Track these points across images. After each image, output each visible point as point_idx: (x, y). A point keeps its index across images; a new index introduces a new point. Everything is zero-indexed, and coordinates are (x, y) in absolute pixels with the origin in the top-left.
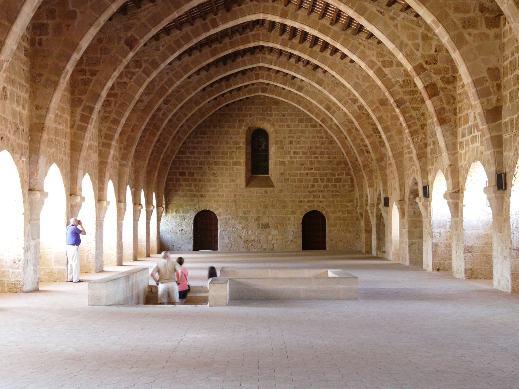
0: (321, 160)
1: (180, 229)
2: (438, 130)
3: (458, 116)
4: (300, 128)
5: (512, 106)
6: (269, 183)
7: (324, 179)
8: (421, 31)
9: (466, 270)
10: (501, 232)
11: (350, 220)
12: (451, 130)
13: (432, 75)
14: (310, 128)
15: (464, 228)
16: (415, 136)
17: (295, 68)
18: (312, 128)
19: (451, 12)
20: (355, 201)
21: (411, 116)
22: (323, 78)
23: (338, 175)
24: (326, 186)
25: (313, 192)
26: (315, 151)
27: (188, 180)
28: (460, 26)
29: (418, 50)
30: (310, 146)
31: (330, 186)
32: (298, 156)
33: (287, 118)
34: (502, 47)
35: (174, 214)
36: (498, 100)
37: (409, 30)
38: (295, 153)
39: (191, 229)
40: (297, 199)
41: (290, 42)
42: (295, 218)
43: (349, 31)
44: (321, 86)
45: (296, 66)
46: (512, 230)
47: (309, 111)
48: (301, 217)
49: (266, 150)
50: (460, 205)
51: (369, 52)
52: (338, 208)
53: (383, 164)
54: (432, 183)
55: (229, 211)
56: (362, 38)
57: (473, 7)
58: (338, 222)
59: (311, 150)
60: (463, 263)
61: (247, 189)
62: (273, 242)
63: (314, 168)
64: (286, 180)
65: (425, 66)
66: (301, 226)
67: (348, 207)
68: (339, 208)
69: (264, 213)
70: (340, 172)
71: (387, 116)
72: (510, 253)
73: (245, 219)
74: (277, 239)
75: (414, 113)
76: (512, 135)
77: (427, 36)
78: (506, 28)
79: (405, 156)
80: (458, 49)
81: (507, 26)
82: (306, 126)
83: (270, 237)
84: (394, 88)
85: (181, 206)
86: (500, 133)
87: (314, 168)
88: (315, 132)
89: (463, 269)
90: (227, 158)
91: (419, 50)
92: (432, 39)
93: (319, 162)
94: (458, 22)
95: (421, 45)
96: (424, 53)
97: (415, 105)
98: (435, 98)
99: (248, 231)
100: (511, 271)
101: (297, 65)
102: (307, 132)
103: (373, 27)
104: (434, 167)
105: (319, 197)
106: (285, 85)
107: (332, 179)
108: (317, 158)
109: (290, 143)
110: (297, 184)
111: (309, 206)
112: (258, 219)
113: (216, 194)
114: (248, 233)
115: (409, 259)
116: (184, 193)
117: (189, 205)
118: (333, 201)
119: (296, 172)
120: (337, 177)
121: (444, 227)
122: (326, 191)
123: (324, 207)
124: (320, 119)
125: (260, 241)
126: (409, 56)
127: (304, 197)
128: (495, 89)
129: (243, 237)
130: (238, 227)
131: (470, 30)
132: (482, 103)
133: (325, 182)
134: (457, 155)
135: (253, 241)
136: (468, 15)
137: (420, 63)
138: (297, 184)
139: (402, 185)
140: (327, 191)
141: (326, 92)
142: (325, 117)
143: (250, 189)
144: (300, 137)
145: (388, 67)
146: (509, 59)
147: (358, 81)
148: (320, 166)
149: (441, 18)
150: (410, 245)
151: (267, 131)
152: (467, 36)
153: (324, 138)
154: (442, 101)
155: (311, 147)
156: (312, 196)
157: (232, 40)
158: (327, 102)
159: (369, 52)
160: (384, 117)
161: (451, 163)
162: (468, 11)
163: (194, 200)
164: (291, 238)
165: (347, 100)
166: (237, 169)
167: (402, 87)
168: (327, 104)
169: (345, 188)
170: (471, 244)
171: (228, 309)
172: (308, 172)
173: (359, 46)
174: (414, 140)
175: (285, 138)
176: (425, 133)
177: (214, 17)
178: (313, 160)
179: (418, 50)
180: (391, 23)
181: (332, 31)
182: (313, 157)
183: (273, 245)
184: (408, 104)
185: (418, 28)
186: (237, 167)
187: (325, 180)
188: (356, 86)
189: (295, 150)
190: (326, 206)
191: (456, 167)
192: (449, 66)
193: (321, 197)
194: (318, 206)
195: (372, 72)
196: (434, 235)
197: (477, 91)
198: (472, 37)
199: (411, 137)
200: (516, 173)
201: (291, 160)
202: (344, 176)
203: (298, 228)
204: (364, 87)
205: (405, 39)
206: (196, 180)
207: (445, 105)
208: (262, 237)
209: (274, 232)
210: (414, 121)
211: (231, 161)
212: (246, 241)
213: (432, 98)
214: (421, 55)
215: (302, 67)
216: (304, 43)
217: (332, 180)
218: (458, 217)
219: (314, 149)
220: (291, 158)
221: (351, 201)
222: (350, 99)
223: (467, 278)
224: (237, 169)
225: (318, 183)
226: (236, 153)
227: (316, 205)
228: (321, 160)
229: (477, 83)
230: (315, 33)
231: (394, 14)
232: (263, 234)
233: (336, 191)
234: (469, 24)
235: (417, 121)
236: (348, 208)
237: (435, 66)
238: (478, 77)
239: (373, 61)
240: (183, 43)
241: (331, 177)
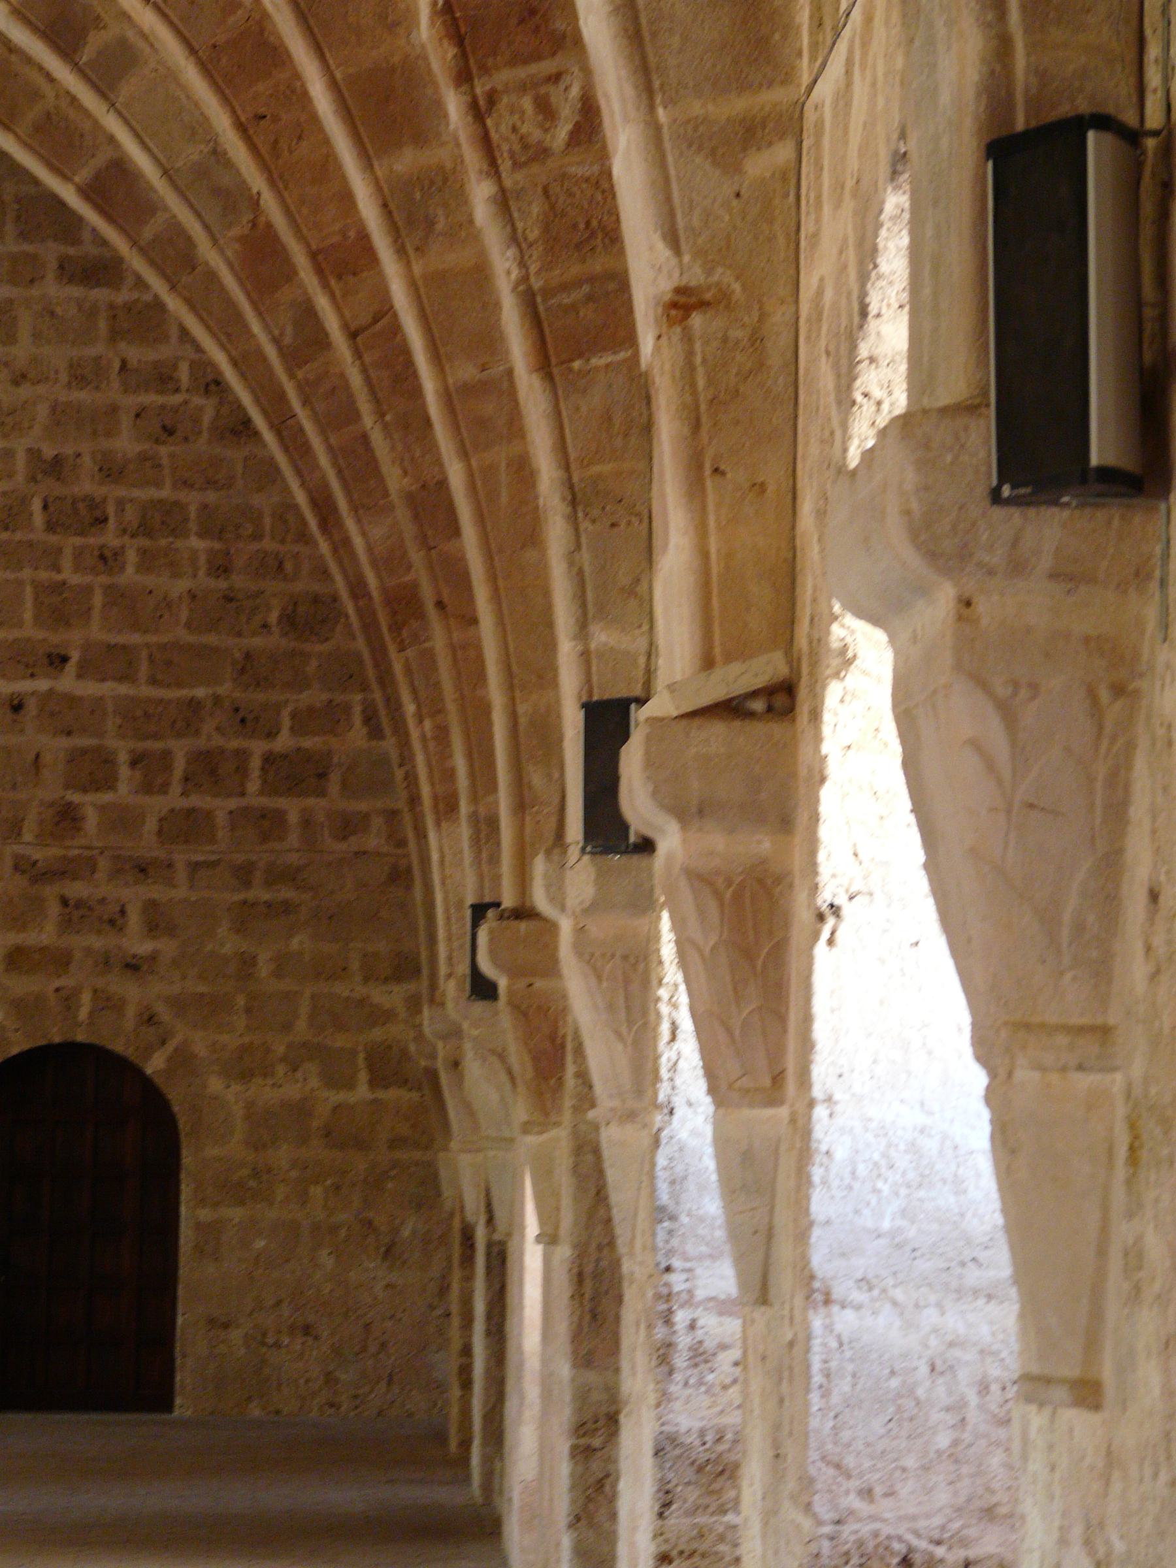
0: (149, 580)
7: (167, 755)
11: (396, 1142)
14: (52, 289)
15: (819, 1259)
16: (504, 76)
18: (76, 291)
23: (303, 722)
26: (94, 504)
30: (49, 452)
31: (221, 818)
52: (287, 1027)
58: (282, 1155)
59: (59, 490)
63: (75, 656)
67: (385, 1016)
68: (301, 1024)
70: (314, 696)
87: (75, 656)
88: (102, 324)
93: (114, 595)
102: (25, 323)
105: (116, 922)
107: (242, 756)
118: (248, 962)
120: (284, 742)
122: (181, 874)
123: (165, 1014)
124: (84, 175)
133: (176, 788)
134: (783, 153)
140: (195, 867)
148: (135, 638)
155: (58, 461)
156: (54, 909)
161: (696, 276)
169: (354, 843)
172: (25, 686)
174: (500, 126)
178: (75, 579)
182: (78, 554)
187: (179, 766)
190: (179, 1004)
191: (757, 339)
193: (134, 919)
194: (107, 1003)
196: (683, 1341)
217: (242, 770)
219: (86, 486)
225: (106, 797)
227: (86, 998)
228: (149, 580)
233: (278, 876)
236: (377, 1034)
241: (234, 744)
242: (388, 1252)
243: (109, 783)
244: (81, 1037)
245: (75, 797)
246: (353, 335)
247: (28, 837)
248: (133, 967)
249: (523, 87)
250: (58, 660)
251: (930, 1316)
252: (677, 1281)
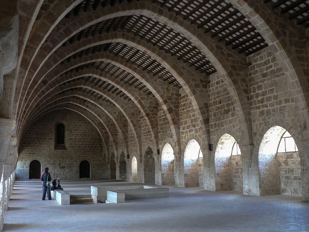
1: (23, 169)
2: (172, 127)
3: (180, 121)
4: (79, 124)
5: (215, 118)
6: (65, 148)
8: (166, 87)
9: (185, 184)
10: (209, 168)
13: (170, 104)
17: (90, 97)
19: (191, 81)
20: (103, 156)
21: (152, 120)
22: (102, 103)
24: (90, 150)
25: (85, 152)
27: (27, 146)
28: (194, 86)
29: (165, 94)
32: (78, 136)
33: (73, 119)
34: (209, 96)
35: (20, 162)
36: (208, 116)
38: (77, 135)
39: (28, 169)
40: (78, 155)
41: (95, 87)
43: (128, 84)
47: (87, 117)
48: (80, 163)
49: (64, 133)
50: (182, 157)
51: (135, 93)
53: (126, 140)
54: (162, 149)
55: (46, 161)
57: (198, 80)
60: (184, 181)
61: (55, 150)
62: (66, 175)
64: (73, 147)
65: (168, 101)
66: (79, 167)
67: (100, 159)
69: (63, 162)
71: (135, 120)
73: (54, 164)
75: (153, 119)
76: (216, 129)
77: (168, 89)
78: (210, 89)
79: (142, 137)
80: (194, 95)
81: (211, 88)
82: (82, 123)
83: (65, 173)
85: (24, 158)
89: (184, 183)
90: (46, 136)
92: (170, 90)
94: (193, 85)
95: (166, 92)
97: (154, 116)
98: (171, 113)
104: (163, 142)
105: (87, 154)
106: (81, 104)
110: (77, 148)
111: (83, 159)
112: (59, 164)
113: (41, 152)
115: (144, 180)
116: (25, 152)
117: (28, 158)
118: (93, 156)
121: (166, 166)
126: (162, 96)
127: (80, 155)
128: (207, 111)
131: (197, 88)
132: (202, 117)
135: (57, 174)
136: (196, 83)
138: (77, 148)
139: (141, 149)
141: (103, 109)
142: (94, 119)
144: (79, 128)
145: (143, 100)
146: (213, 100)
149: (188, 83)
150: (145, 174)
152: (196, 90)
153: (90, 128)
154: (174, 115)
157: (69, 84)
158: (99, 113)
159: (135, 93)
160: (134, 120)
162: (196, 81)
163: (30, 155)
165: (112, 113)
166: (51, 142)
167: (148, 108)
168: (99, 114)
170: (187, 173)
171: (70, 206)
175: (73, 128)
176: (157, 128)
177: (71, 73)
179: (165, 94)
180: (155, 83)
181: (121, 83)
184: (151, 115)
185: (165, 85)
188: (122, 107)
189: (77, 133)
192: (176, 101)
193: (88, 154)
197: (201, 112)
198: (198, 91)
199: (152, 129)
202: (98, 145)
203: (78, 168)
204: (125, 108)
205: (160, 89)
206: (31, 146)
208: (62, 173)
209: (67, 170)
210: (153, 122)
211: (48, 138)
215: (93, 97)
216: (101, 87)
218: (180, 162)
220: (75, 137)
221: (101, 156)
222: (113, 112)
224: (51, 142)
226: (50, 134)
229: (201, 109)
230: (113, 84)
231: (156, 79)
234: (197, 86)
235: (154, 122)
237: (172, 101)
238: (201, 106)
239: (137, 97)
240: (56, 83)
242: (100, 170)
243: (87, 148)
248: (88, 156)
250: (84, 142)
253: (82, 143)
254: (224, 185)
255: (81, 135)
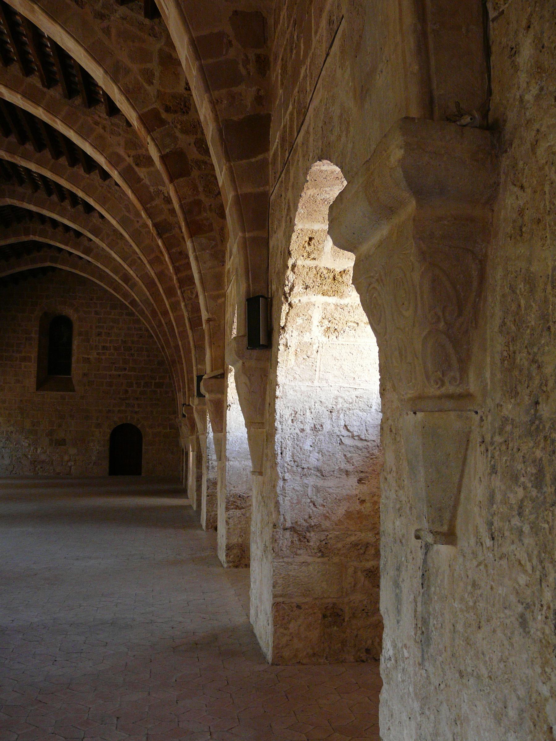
6: (68, 386)
8: (158, 46)
12: (213, 248)
13: (178, 134)
29: (151, 83)
36: (259, 100)
37: (133, 42)
42: (100, 433)
44: (97, 237)
45: (61, 206)
46: (279, 469)
47: (114, 289)
48: (110, 431)
55: (12, 422)
56: (101, 115)
62: (69, 464)
65: (164, 115)
72: (274, 540)
74: (75, 460)
83: (66, 458)
84: (154, 203)
86: (262, 189)
88: (132, 322)
90: (13, 352)
91: (152, 83)
95: (157, 74)
96: (163, 90)
99: (37, 449)
100: (275, 596)
101: (62, 204)
103: (59, 28)
107: (152, 382)
108: (132, 355)
109: (99, 335)
114: (36, 451)
119: (106, 373)
120: (157, 381)
125: (52, 462)
129: (29, 456)
130: (23, 444)
134: (223, 299)
135: (43, 462)
137: (155, 108)
143: (42, 393)
147: (128, 214)
151: (72, 318)
154: (195, 188)
161: (211, 316)
164: (94, 458)
173: (95, 126)
175: (91, 327)
178: (127, 357)
179: (151, 83)
183: (70, 467)
186: (26, 364)
187: (142, 384)
189: (105, 344)
191: (219, 325)
195: (116, 172)
196: (211, 465)
200: (291, 289)
201: (98, 356)
207: (202, 197)
209: (73, 451)
212: (33, 462)
213: (176, 181)
214: (156, 94)
220: (98, 354)
223: (230, 564)
225: (132, 388)
227: (129, 417)
232: (58, 453)
237: (184, 118)
239: (119, 156)
244: (129, 422)
245: (128, 389)
246: (166, 324)
247: (121, 394)
248: (136, 413)
249: (188, 290)
250: (125, 369)
251: (243, 462)
252: (210, 457)
253: (117, 373)
254: (354, 616)
255: (116, 349)
